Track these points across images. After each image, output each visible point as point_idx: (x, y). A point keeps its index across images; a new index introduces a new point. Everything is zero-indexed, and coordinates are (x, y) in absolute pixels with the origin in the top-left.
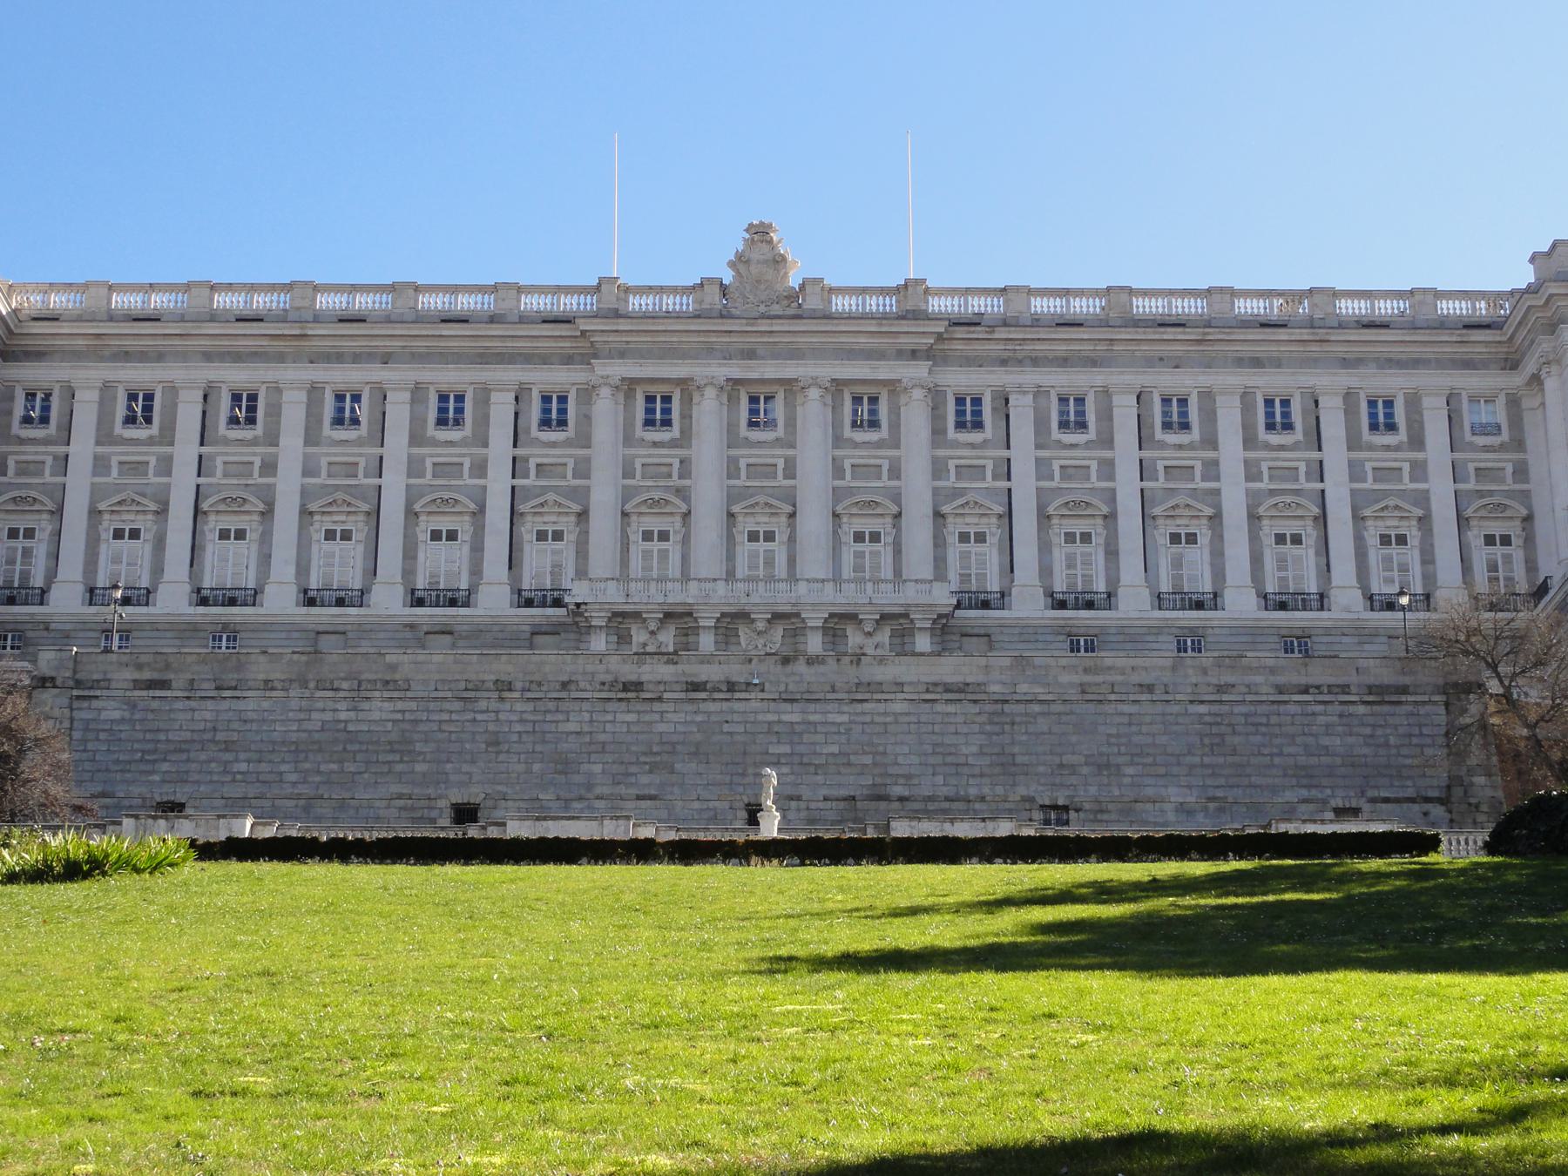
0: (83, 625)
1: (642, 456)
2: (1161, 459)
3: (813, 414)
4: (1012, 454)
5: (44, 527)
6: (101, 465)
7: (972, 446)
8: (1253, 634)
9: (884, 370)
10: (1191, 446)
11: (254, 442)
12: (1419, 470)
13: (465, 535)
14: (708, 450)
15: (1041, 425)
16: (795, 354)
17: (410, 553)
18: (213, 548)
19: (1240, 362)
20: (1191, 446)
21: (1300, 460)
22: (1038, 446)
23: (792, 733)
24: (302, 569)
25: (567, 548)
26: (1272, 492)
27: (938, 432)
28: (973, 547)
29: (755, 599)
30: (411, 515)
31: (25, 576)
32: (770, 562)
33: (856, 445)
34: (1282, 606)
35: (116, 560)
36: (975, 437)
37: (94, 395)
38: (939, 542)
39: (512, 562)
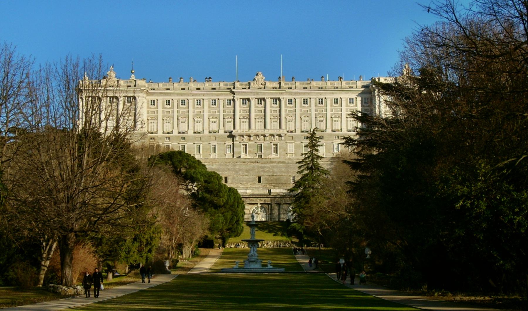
0: (163, 136)
2: (318, 109)
4: (297, 108)
5: (156, 121)
6: (163, 112)
7: (290, 107)
8: (330, 135)
10: (323, 107)
11: (185, 108)
13: (217, 122)
16: (264, 94)
18: (181, 124)
19: (330, 93)
20: (323, 107)
21: (339, 109)
22: (300, 107)
23: (263, 168)
24: (194, 127)
26: (334, 114)
27: (286, 105)
28: (290, 123)
29: (259, 133)
31: (154, 129)
32: (261, 125)
33: (273, 107)
34: (335, 131)
35: (167, 126)
36: (291, 106)
37: (161, 101)
38: (286, 122)
39: (224, 126)
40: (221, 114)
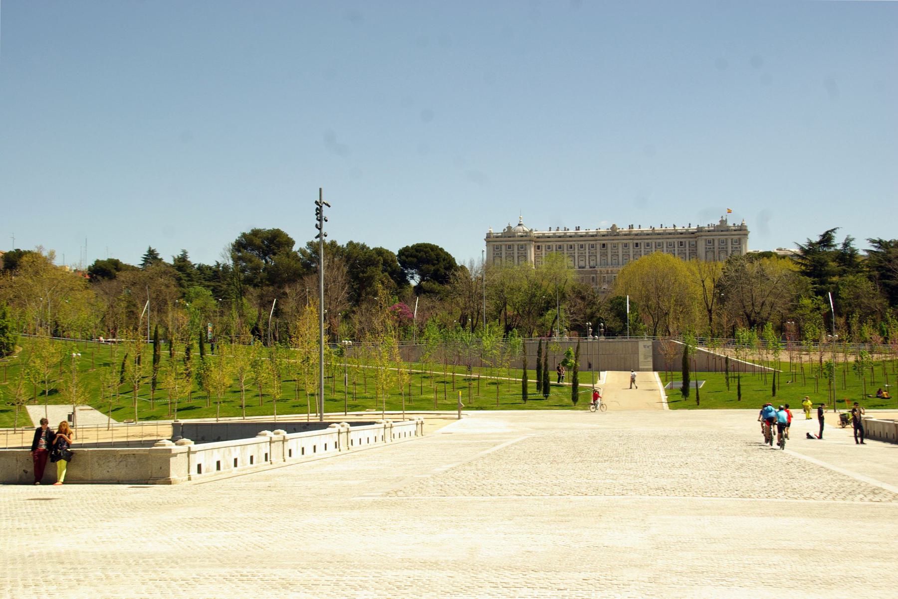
1: (603, 251)
3: (620, 246)
9: (628, 241)
12: (685, 250)
14: (609, 250)
15: (645, 246)
17: (578, 262)
25: (595, 261)
27: (633, 247)
30: (578, 259)
40: (587, 254)
